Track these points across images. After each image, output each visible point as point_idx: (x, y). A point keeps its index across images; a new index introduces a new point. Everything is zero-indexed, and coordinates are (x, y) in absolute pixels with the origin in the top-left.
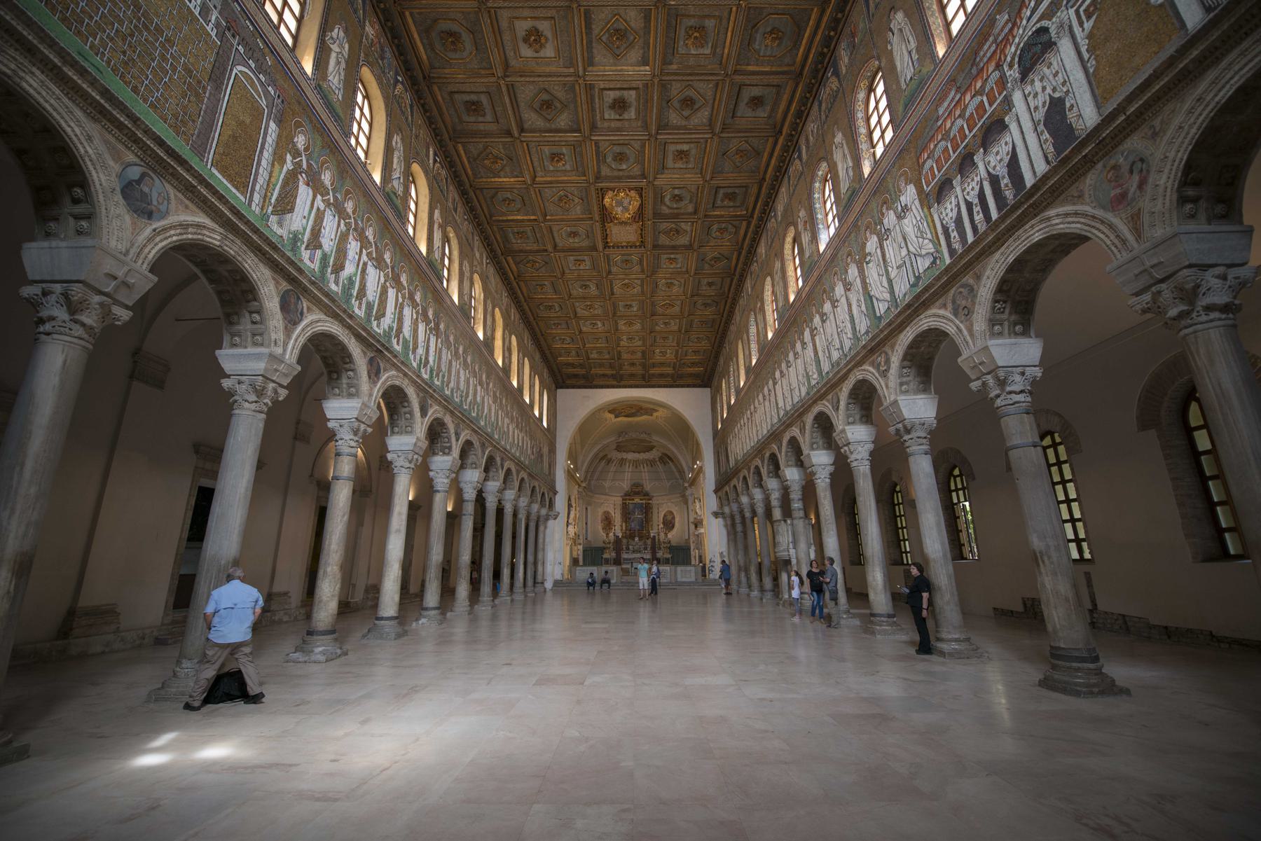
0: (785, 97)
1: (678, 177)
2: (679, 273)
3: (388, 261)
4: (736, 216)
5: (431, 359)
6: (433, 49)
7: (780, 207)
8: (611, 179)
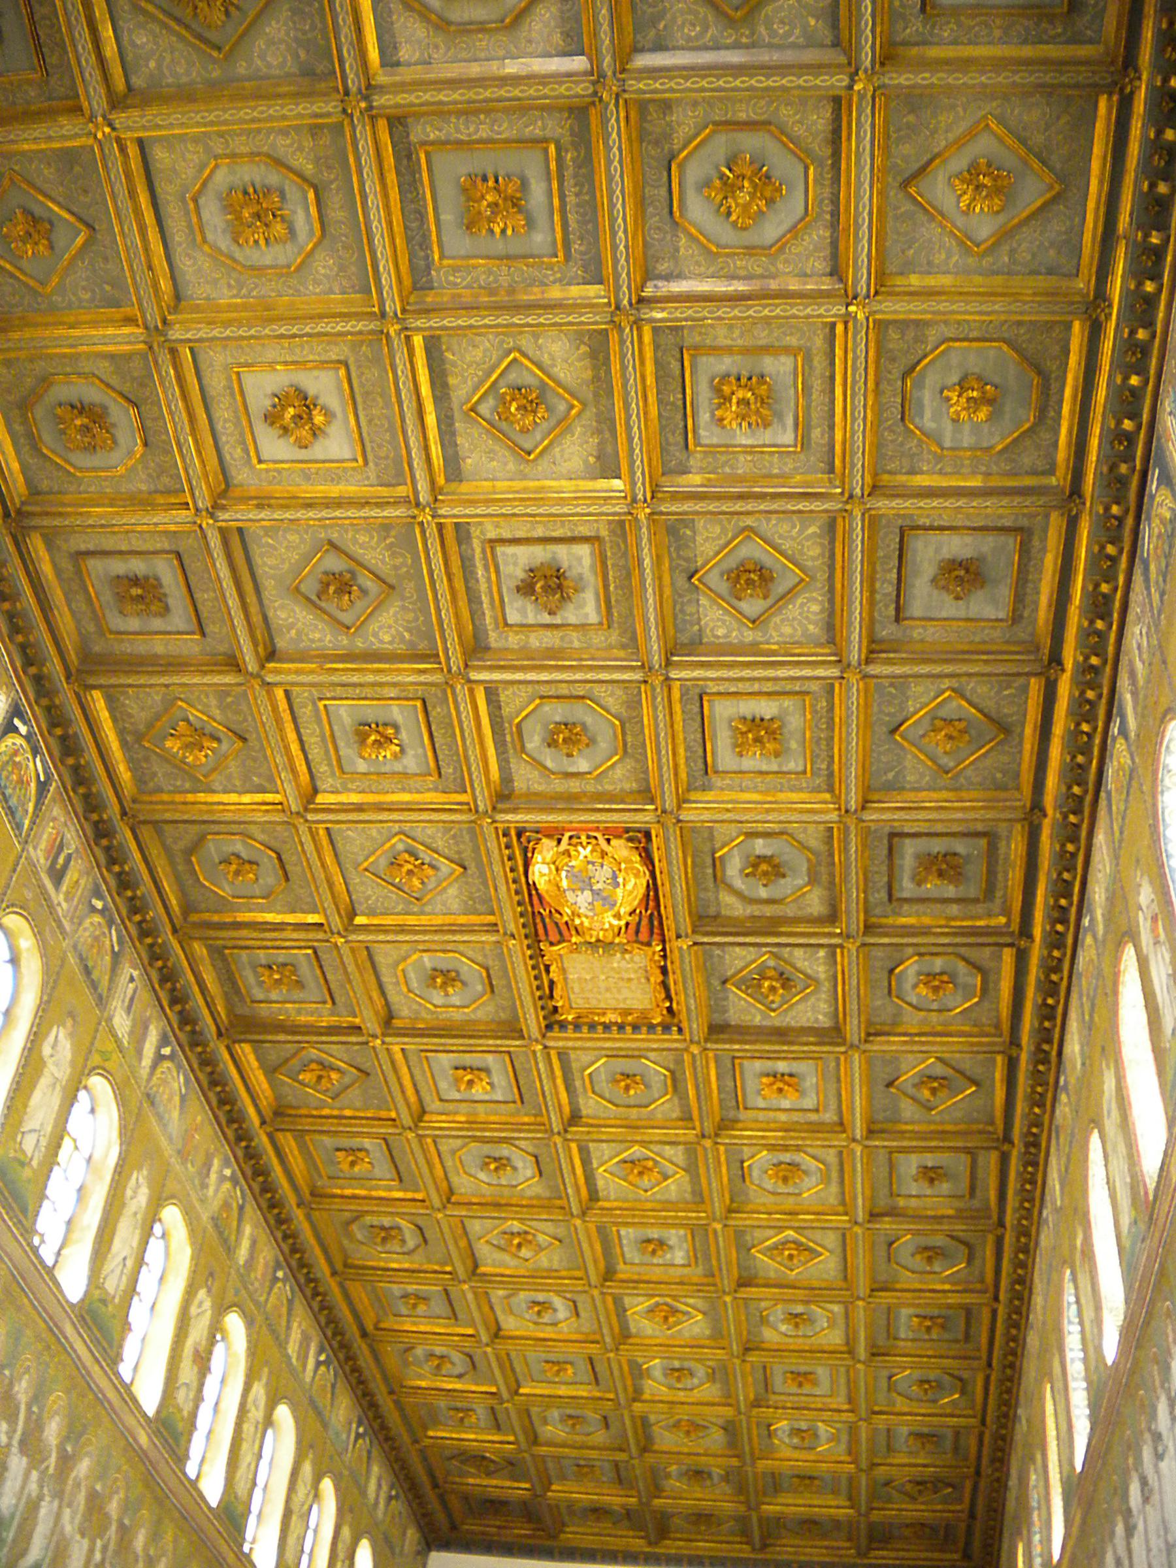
0: (1050, 562)
1: (757, 801)
2: (816, 1128)
4: (974, 932)
6: (36, 449)
7: (1098, 894)
8: (549, 802)
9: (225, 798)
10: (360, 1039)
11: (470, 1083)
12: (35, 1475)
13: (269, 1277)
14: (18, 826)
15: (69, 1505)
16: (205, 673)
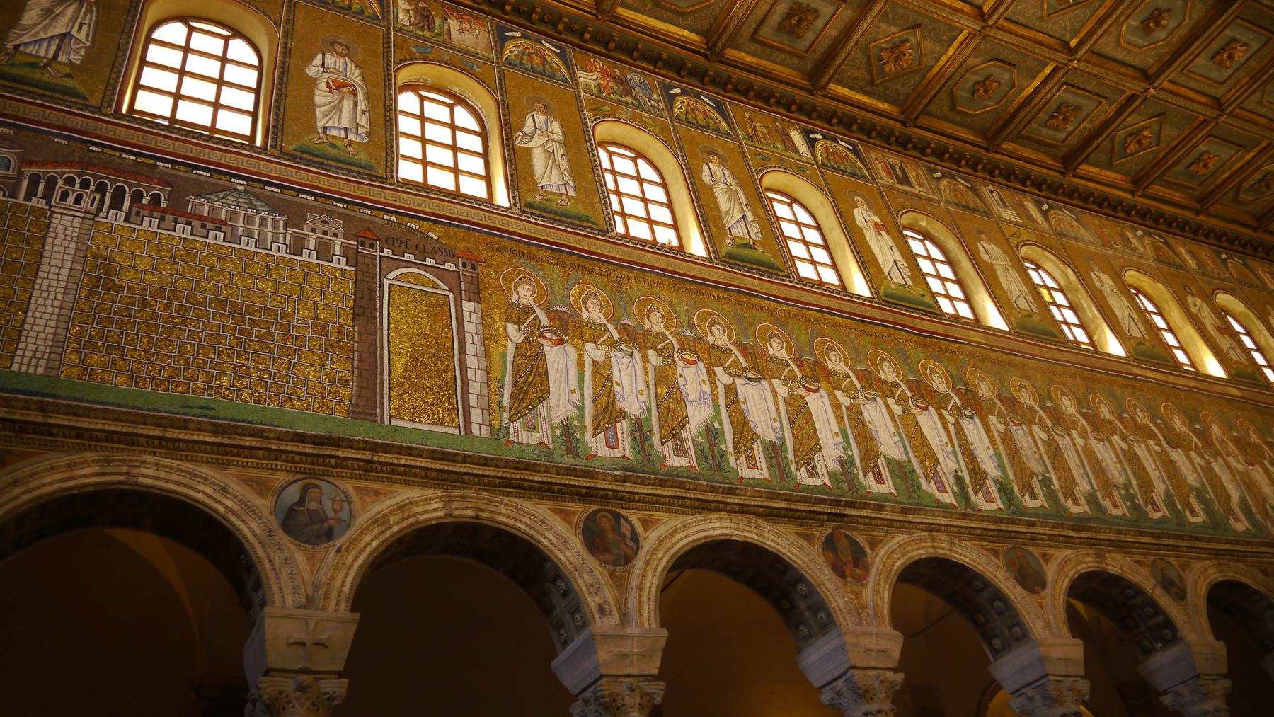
3: (782, 354)
5: (990, 467)
9: (941, 63)
10: (1140, 100)
11: (1231, 57)
12: (1193, 454)
13: (1219, 262)
14: (863, 177)
15: (1228, 455)
16: (866, 16)
